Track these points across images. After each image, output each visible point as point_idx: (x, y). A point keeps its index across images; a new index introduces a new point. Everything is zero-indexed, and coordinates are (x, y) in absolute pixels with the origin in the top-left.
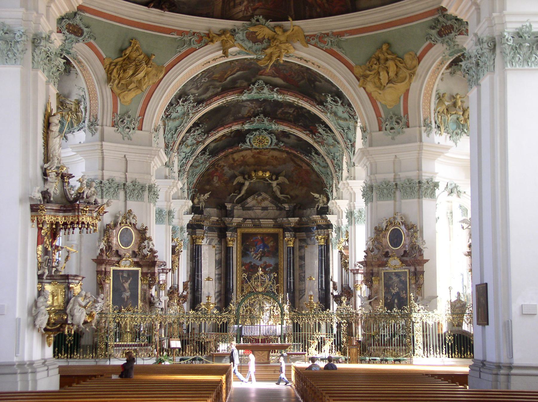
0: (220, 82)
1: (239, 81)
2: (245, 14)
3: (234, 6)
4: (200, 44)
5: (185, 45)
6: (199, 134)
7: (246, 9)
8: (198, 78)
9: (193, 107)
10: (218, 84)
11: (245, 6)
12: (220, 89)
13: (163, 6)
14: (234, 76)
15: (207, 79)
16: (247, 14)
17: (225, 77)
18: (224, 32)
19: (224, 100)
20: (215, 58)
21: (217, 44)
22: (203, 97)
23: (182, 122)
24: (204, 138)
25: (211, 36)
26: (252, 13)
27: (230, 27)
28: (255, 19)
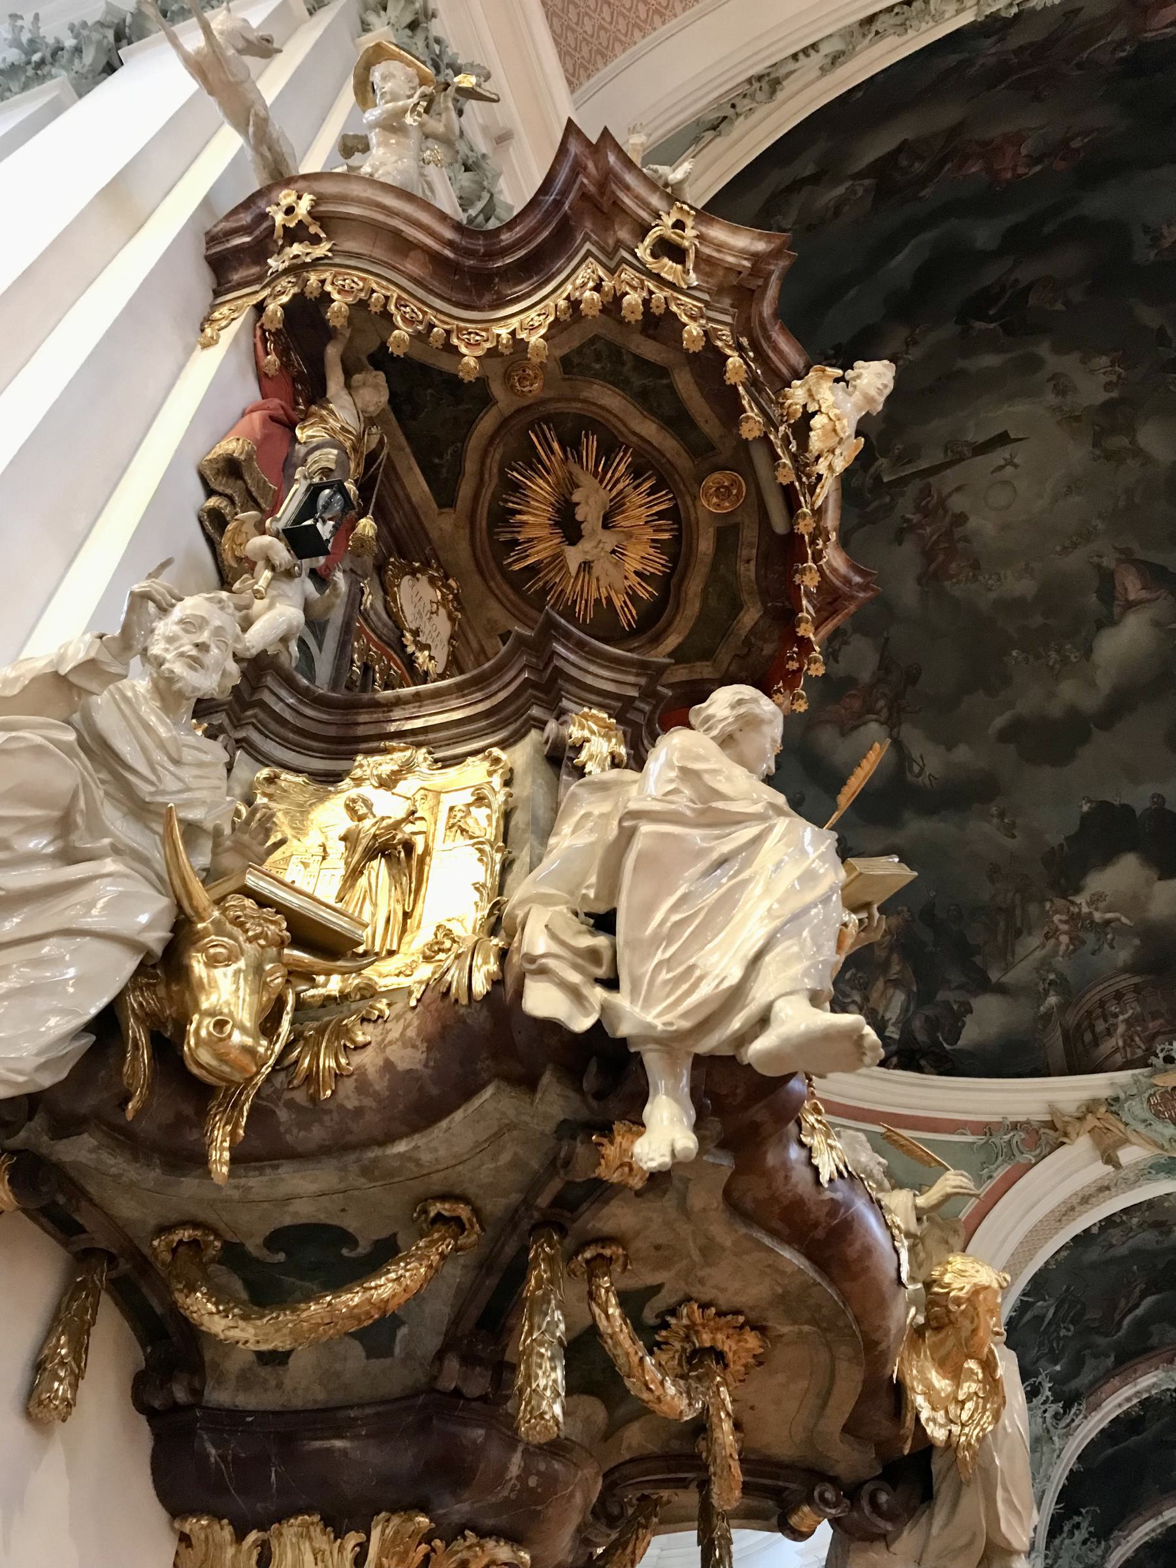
0: (1107, 1336)
1: (1154, 1328)
2: (1129, 1055)
3: (1096, 1042)
4: (1038, 1151)
5: (1000, 1158)
6: (1084, 1542)
7: (1129, 1041)
8: (1049, 1324)
9: (1057, 1417)
10: (1101, 1341)
11: (1123, 1036)
12: (1112, 1358)
13: (923, 1062)
14: (1139, 1312)
15: (1072, 1328)
16: (1133, 1053)
17: (1117, 1317)
18: (1090, 1107)
19: (1128, 1391)
20: (1087, 1192)
21: (1081, 1147)
22: (1075, 1384)
23: (1041, 1465)
24: (1099, 1552)
25: (1059, 1125)
26: (1147, 1050)
27: (1106, 1093)
28: (1161, 1055)
